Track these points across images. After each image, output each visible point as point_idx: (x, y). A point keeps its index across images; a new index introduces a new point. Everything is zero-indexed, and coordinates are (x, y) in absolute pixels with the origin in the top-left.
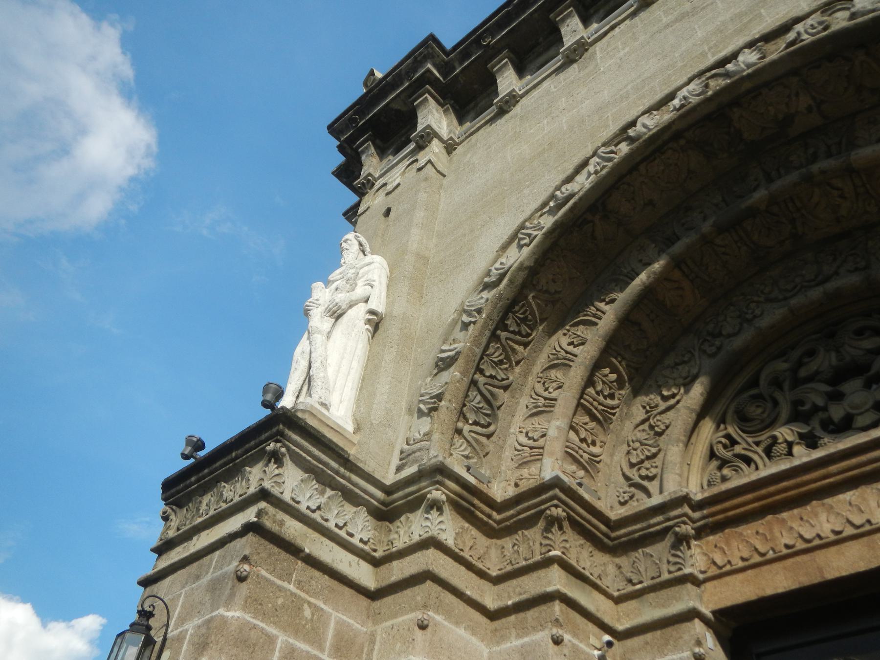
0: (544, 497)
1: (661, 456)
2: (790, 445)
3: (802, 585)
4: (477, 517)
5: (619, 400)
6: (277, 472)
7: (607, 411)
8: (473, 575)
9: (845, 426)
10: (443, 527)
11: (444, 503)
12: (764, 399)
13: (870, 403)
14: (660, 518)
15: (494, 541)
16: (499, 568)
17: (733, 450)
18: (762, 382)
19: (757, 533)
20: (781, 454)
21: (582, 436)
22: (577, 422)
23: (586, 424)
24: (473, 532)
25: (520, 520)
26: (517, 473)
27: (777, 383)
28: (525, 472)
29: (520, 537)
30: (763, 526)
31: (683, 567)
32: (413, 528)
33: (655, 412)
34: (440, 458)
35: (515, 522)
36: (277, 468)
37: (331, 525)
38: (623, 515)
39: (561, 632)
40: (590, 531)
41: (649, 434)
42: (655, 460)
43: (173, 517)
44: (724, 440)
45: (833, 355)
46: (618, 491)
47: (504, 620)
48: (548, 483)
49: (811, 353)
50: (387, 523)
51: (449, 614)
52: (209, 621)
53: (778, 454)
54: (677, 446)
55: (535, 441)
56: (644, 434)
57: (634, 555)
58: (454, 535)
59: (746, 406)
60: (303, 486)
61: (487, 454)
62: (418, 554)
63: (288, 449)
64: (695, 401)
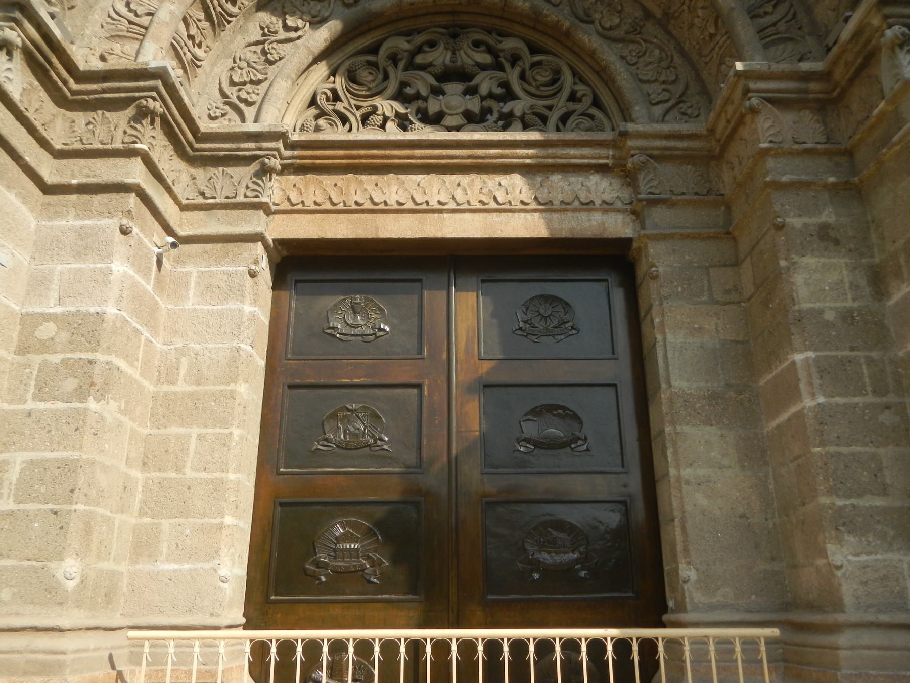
0: (141, 84)
1: (265, 85)
2: (386, 119)
3: (358, 237)
4: (50, 78)
5: (240, 9)
7: (223, 16)
8: (34, 141)
9: (434, 120)
12: (378, 68)
14: (252, 145)
15: (62, 111)
16: (63, 142)
17: (335, 105)
18: (383, 52)
19: (336, 185)
20: (375, 124)
21: (192, 33)
22: (192, 15)
23: (200, 21)
25: (103, 98)
26: (106, 45)
28: (117, 47)
29: (98, 117)
30: (342, 181)
31: (260, 196)
33: (273, 38)
35: (96, 99)
38: (214, 131)
39: (131, 224)
40: (177, 134)
41: (260, 58)
42: (258, 87)
44: (329, 93)
45: (449, 54)
46: (210, 104)
47: (61, 197)
48: (152, 70)
49: (432, 44)
53: (373, 123)
54: (286, 81)
55: (136, 15)
56: (255, 56)
57: (212, 171)
58: (21, 90)
59: (359, 68)
61: (72, 7)
64: (318, 44)
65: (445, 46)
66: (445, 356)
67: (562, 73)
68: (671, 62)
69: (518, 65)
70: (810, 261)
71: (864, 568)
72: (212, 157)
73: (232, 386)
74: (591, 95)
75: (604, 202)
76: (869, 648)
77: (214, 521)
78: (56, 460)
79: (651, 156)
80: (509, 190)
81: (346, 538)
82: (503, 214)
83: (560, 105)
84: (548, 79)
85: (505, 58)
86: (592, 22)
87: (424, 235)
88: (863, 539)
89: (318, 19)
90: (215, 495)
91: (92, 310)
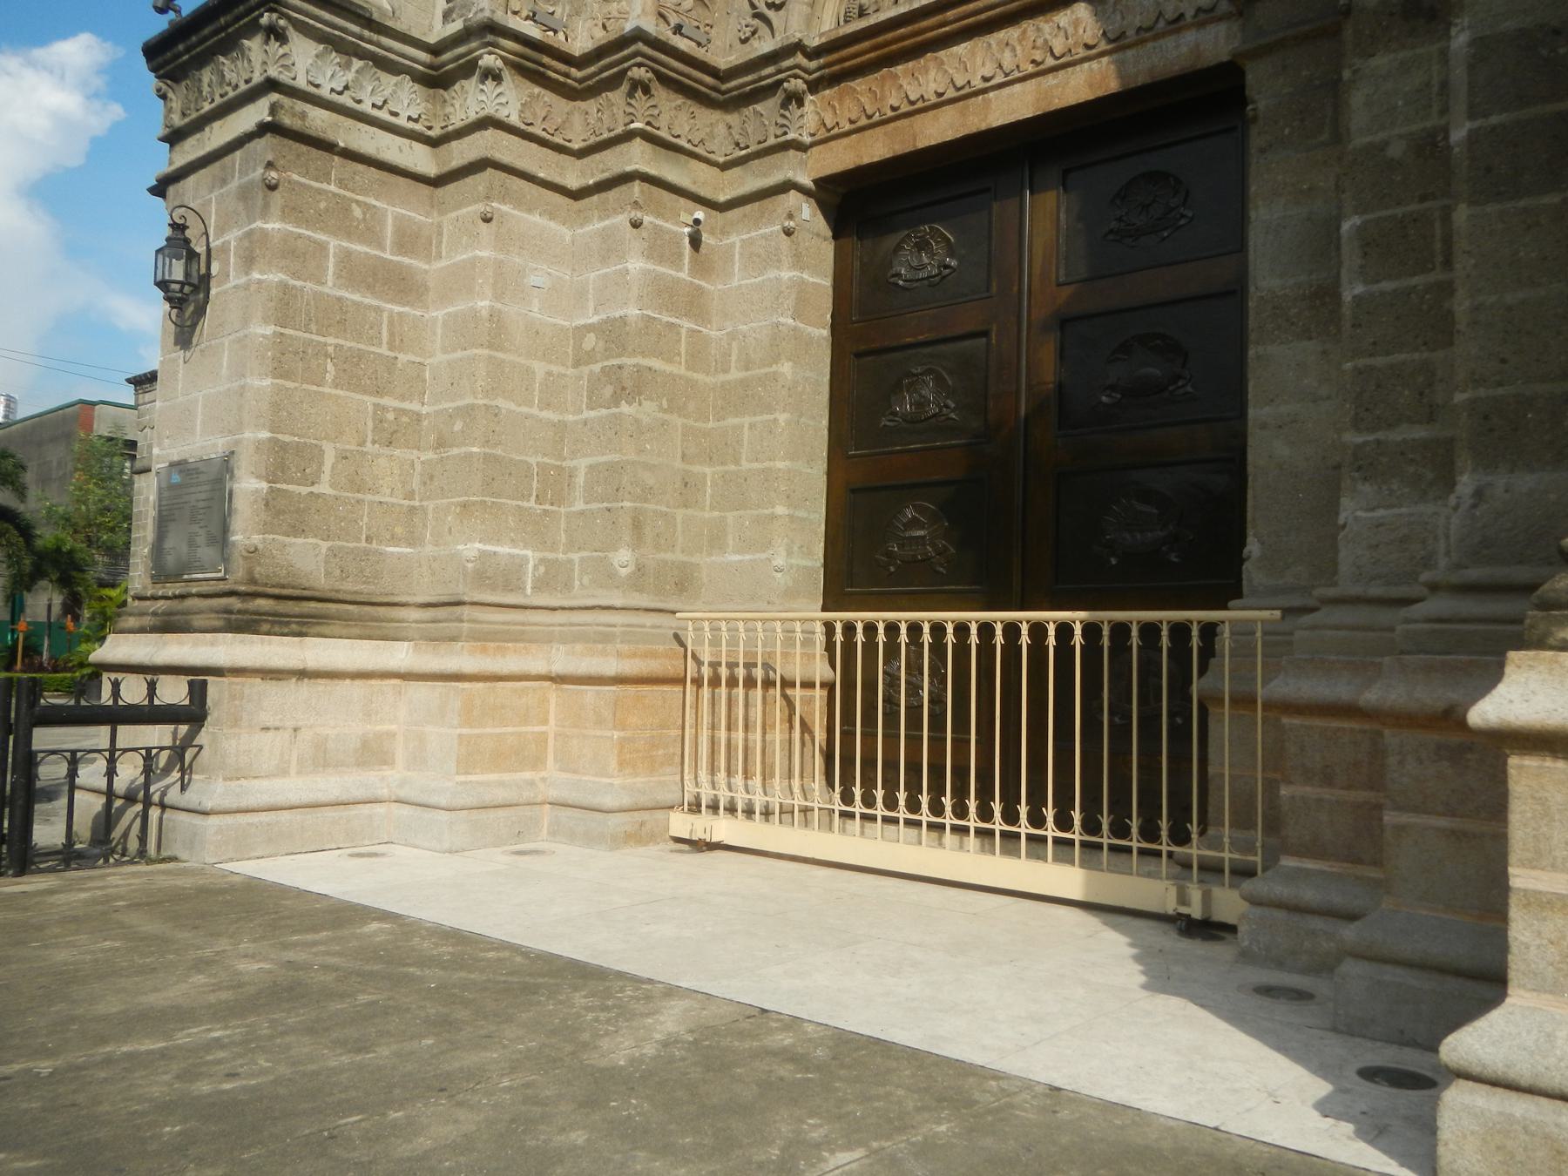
0: (626, 52)
4: (549, 78)
6: (281, 51)
8: (550, 151)
10: (503, 100)
11: (500, 70)
24: (546, 99)
25: (602, 80)
32: (468, 100)
34: (487, 14)
36: (280, 46)
37: (366, 107)
39: (639, 215)
43: (170, 95)
47: (587, 200)
50: (441, 91)
51: (519, 203)
52: (249, 234)
58: (519, 106)
60: (320, 63)
62: (477, 135)
63: (289, 18)
66: (1015, 289)
70: (1381, 62)
71: (1377, 527)
72: (740, 96)
73: (774, 368)
75: (1199, 10)
76: (1337, 628)
77: (766, 511)
78: (606, 463)
80: (1070, 31)
81: (914, 523)
82: (1061, 73)
87: (967, 132)
88: (1384, 487)
90: (766, 485)
91: (617, 316)
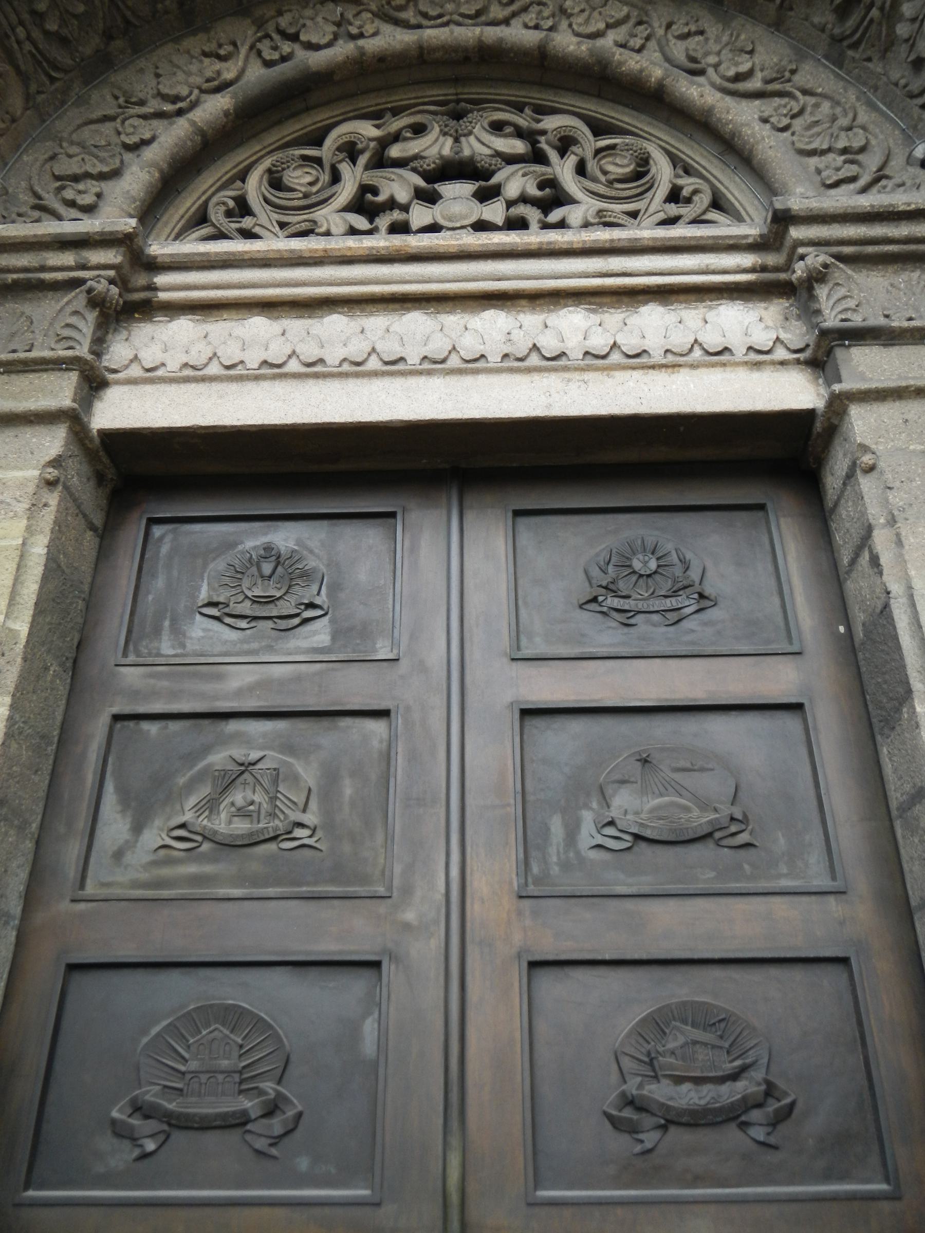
13: (473, 219)
14: (68, 258)
18: (330, 142)
27: (351, 151)
44: (231, 204)
45: (449, 141)
49: (419, 130)
59: (288, 167)
65: (441, 131)
67: (651, 162)
68: (854, 119)
69: (573, 153)
74: (709, 192)
79: (840, 258)
83: (652, 209)
84: (628, 170)
85: (548, 143)
86: (701, 72)
89: (216, 83)
